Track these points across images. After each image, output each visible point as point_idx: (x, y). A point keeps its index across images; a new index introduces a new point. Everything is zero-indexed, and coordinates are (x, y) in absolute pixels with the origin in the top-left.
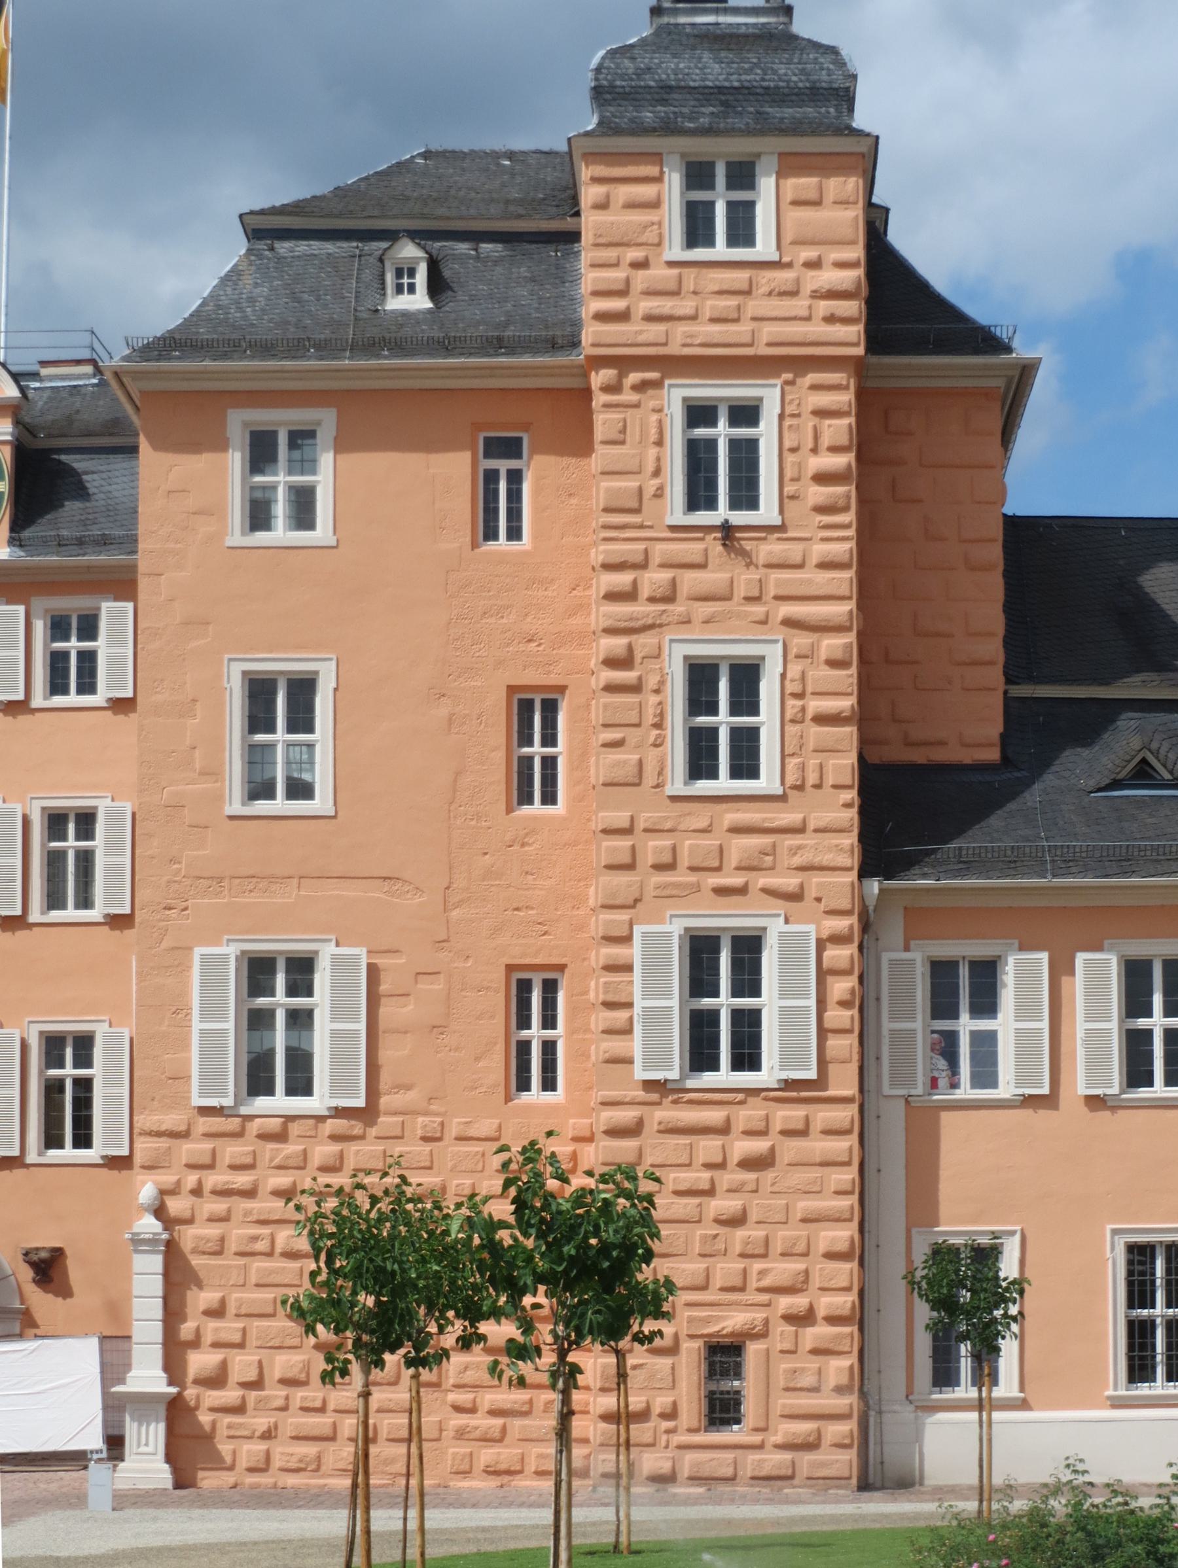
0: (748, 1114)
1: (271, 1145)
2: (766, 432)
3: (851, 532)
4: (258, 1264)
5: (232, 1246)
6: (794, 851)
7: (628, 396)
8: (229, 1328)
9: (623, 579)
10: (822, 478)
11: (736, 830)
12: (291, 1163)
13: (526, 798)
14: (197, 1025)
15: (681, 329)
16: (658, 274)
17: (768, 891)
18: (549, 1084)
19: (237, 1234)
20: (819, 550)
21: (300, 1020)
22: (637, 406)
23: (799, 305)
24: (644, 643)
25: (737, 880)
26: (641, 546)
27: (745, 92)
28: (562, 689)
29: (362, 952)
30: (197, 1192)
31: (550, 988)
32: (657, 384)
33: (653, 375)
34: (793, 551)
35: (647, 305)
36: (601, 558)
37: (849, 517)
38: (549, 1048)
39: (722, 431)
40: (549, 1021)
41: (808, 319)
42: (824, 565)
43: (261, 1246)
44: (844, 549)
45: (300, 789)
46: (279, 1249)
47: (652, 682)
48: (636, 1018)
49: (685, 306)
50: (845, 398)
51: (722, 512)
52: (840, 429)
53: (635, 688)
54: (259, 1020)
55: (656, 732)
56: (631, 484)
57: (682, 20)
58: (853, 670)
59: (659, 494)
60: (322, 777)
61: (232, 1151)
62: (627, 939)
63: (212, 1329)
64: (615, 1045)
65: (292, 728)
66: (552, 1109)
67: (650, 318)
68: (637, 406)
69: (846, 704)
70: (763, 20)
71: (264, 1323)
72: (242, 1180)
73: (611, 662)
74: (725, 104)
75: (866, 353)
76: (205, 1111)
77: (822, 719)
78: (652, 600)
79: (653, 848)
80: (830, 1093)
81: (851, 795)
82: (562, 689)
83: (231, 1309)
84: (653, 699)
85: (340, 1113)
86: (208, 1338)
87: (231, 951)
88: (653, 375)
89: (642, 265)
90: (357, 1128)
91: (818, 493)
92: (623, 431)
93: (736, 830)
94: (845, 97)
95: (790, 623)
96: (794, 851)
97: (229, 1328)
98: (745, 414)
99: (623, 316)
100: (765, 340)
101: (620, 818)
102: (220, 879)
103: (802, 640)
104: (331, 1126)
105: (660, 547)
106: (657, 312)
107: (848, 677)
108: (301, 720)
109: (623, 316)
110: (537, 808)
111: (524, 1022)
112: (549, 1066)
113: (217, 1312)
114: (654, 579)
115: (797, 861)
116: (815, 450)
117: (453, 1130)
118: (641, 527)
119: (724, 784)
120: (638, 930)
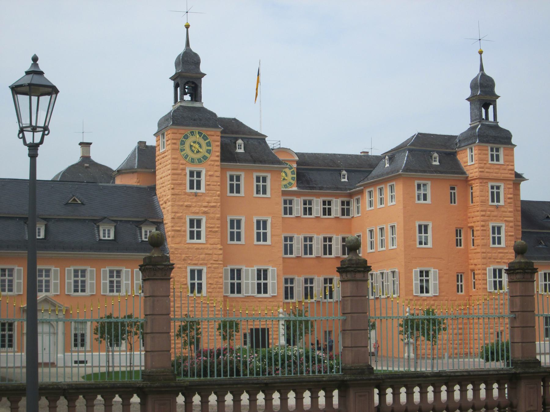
2: (502, 191)
6: (507, 256)
9: (483, 213)
11: (500, 253)
13: (457, 246)
15: (491, 174)
16: (488, 165)
17: (503, 262)
18: (462, 291)
21: (427, 281)
22: (484, 186)
23: (506, 171)
24: (487, 223)
25: (499, 261)
26: (486, 208)
32: (487, 182)
34: (505, 210)
35: (487, 170)
36: (481, 210)
38: (461, 285)
39: (495, 190)
41: (507, 174)
42: (510, 212)
49: (492, 171)
50: (511, 186)
53: (485, 230)
56: (484, 198)
59: (488, 200)
62: (486, 270)
64: (484, 286)
67: (487, 172)
68: (484, 186)
73: (483, 226)
74: (495, 138)
78: (487, 216)
84: (488, 232)
89: (485, 164)
91: (509, 201)
92: (483, 190)
93: (500, 253)
95: (505, 221)
96: (507, 256)
98: (498, 188)
101: (484, 250)
103: (507, 224)
105: (488, 208)
110: (459, 247)
111: (458, 281)
115: (507, 258)
116: (508, 194)
118: (485, 205)
120: (487, 268)
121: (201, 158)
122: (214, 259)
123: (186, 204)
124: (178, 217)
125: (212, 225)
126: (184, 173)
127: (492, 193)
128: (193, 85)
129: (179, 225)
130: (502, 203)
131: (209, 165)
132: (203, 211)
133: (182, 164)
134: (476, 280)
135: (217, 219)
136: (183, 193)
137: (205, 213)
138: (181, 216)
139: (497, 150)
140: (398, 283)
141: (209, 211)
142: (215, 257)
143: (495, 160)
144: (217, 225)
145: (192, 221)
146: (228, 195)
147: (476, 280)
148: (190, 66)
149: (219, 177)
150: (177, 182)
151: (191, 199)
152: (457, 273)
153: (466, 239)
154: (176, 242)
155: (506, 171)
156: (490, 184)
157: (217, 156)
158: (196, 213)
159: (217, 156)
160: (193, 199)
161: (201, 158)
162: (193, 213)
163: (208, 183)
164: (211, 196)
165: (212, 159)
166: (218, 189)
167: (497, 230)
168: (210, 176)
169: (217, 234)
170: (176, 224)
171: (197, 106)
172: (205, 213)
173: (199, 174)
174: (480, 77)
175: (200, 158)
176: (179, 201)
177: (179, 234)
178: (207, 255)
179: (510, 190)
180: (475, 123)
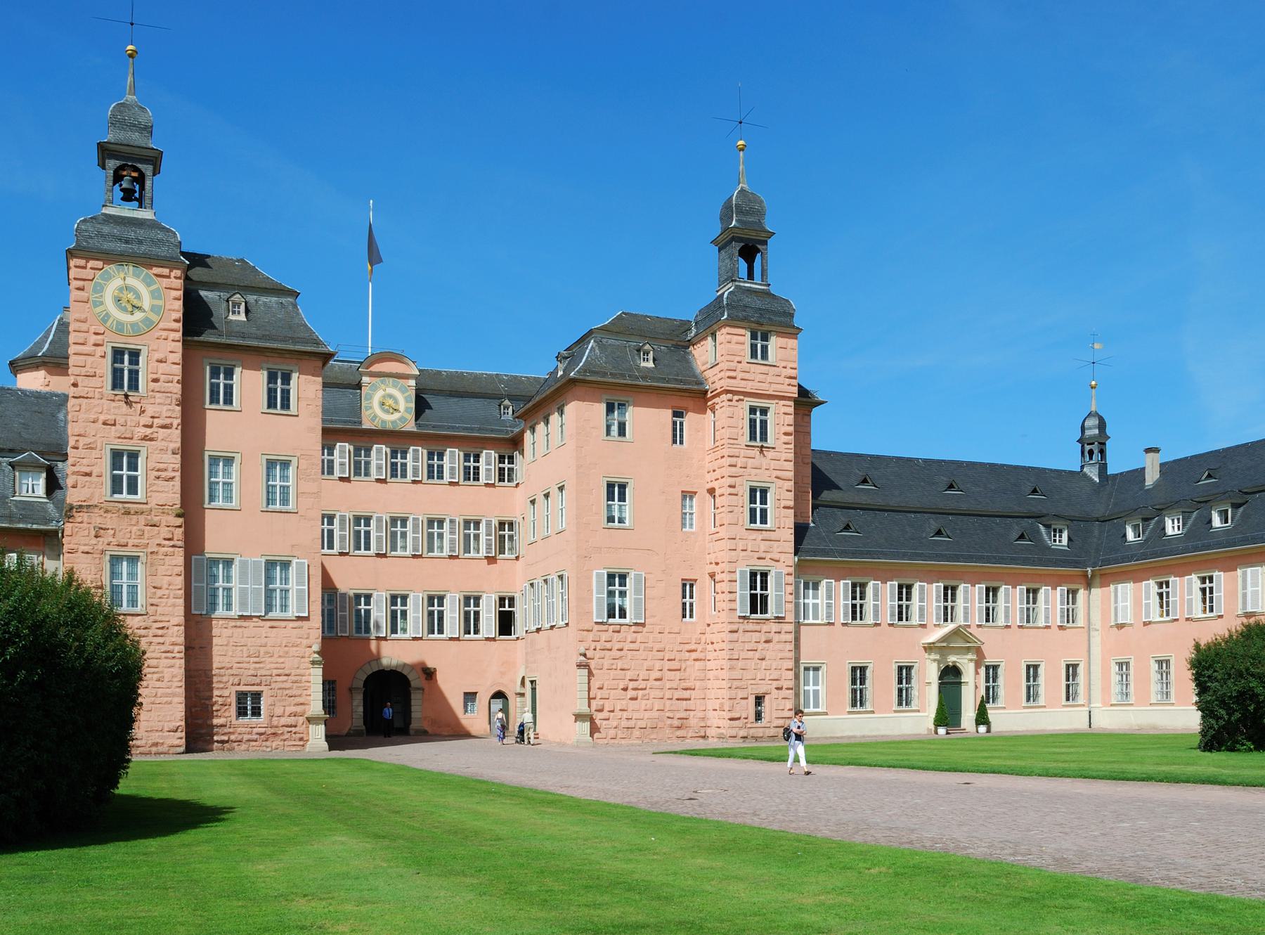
0: (765, 628)
1: (616, 634)
2: (770, 418)
3: (793, 451)
4: (612, 672)
5: (606, 667)
7: (734, 403)
8: (604, 693)
10: (786, 434)
12: (622, 640)
14: (595, 596)
15: (750, 383)
19: (606, 663)
20: (784, 456)
23: (780, 380)
27: (767, 310)
28: (695, 493)
29: (643, 573)
30: (595, 650)
31: (692, 586)
33: (742, 397)
36: (728, 454)
37: (792, 446)
40: (691, 597)
43: (614, 667)
44: (791, 456)
45: (621, 521)
46: (619, 668)
47: (740, 494)
48: (738, 597)
50: (791, 410)
51: (759, 444)
52: (790, 419)
54: (611, 594)
55: (742, 509)
57: (742, 284)
58: (793, 493)
60: (627, 515)
61: (604, 636)
63: (599, 694)
65: (619, 501)
66: (692, 623)
69: (791, 503)
70: (763, 287)
71: (614, 691)
72: (608, 645)
74: (761, 314)
75: (799, 396)
76: (597, 623)
77: (784, 507)
79: (741, 545)
80: (786, 621)
81: (793, 531)
82: (695, 493)
83: (605, 687)
85: (636, 624)
86: (599, 697)
87: (605, 572)
88: (742, 397)
90: (640, 629)
94: (792, 316)
97: (604, 693)
98: (764, 411)
99: (735, 378)
100: (773, 389)
102: (601, 548)
104: (633, 628)
106: (744, 378)
107: (791, 495)
108: (622, 498)
109: (735, 378)
112: (691, 611)
113: (601, 688)
114: (740, 462)
117: (667, 630)
119: (758, 525)
121: (140, 323)
122: (162, 536)
123: (102, 418)
124: (85, 445)
125: (162, 466)
126: (99, 351)
127: (752, 423)
128: (134, 174)
129: (84, 461)
130: (771, 441)
131: (158, 339)
132: (140, 434)
133: (96, 334)
134: (718, 593)
135: (174, 453)
136: (97, 396)
137: (145, 438)
138: (94, 442)
139: (765, 338)
140: (567, 597)
141: (155, 435)
142: (165, 532)
143: (759, 356)
144: (174, 466)
145: (117, 456)
146: (206, 407)
147: (718, 593)
148: (130, 133)
149: (179, 364)
150: (83, 371)
151: (115, 407)
152: (682, 580)
153: (702, 514)
154: (80, 499)
155: (780, 380)
156: (749, 402)
157: (176, 321)
158: (125, 438)
159: (176, 321)
160: (119, 407)
161: (140, 323)
162: (119, 438)
163: (155, 376)
164: (159, 404)
165: (166, 327)
166: (175, 391)
167: (758, 494)
168: (160, 361)
169: (172, 483)
170: (78, 460)
171: (140, 217)
172: (145, 438)
173: (135, 355)
174: (738, 193)
175: (137, 323)
176: (88, 411)
177: (87, 481)
178: (149, 528)
179: (787, 416)
180: (725, 286)
